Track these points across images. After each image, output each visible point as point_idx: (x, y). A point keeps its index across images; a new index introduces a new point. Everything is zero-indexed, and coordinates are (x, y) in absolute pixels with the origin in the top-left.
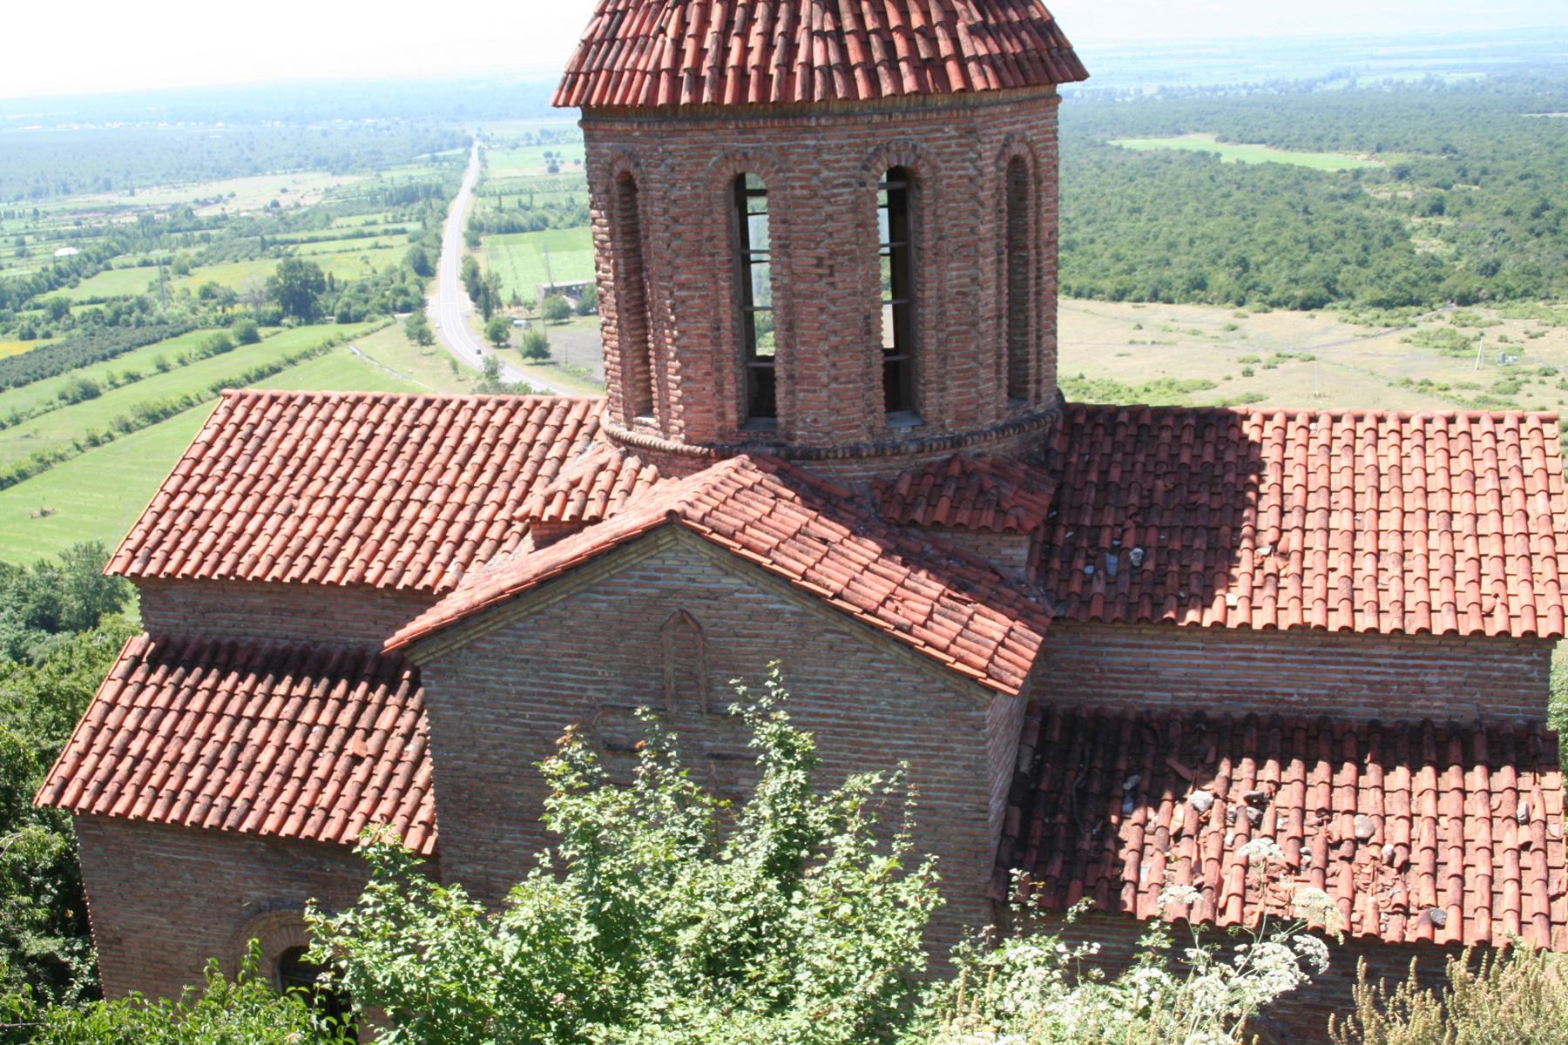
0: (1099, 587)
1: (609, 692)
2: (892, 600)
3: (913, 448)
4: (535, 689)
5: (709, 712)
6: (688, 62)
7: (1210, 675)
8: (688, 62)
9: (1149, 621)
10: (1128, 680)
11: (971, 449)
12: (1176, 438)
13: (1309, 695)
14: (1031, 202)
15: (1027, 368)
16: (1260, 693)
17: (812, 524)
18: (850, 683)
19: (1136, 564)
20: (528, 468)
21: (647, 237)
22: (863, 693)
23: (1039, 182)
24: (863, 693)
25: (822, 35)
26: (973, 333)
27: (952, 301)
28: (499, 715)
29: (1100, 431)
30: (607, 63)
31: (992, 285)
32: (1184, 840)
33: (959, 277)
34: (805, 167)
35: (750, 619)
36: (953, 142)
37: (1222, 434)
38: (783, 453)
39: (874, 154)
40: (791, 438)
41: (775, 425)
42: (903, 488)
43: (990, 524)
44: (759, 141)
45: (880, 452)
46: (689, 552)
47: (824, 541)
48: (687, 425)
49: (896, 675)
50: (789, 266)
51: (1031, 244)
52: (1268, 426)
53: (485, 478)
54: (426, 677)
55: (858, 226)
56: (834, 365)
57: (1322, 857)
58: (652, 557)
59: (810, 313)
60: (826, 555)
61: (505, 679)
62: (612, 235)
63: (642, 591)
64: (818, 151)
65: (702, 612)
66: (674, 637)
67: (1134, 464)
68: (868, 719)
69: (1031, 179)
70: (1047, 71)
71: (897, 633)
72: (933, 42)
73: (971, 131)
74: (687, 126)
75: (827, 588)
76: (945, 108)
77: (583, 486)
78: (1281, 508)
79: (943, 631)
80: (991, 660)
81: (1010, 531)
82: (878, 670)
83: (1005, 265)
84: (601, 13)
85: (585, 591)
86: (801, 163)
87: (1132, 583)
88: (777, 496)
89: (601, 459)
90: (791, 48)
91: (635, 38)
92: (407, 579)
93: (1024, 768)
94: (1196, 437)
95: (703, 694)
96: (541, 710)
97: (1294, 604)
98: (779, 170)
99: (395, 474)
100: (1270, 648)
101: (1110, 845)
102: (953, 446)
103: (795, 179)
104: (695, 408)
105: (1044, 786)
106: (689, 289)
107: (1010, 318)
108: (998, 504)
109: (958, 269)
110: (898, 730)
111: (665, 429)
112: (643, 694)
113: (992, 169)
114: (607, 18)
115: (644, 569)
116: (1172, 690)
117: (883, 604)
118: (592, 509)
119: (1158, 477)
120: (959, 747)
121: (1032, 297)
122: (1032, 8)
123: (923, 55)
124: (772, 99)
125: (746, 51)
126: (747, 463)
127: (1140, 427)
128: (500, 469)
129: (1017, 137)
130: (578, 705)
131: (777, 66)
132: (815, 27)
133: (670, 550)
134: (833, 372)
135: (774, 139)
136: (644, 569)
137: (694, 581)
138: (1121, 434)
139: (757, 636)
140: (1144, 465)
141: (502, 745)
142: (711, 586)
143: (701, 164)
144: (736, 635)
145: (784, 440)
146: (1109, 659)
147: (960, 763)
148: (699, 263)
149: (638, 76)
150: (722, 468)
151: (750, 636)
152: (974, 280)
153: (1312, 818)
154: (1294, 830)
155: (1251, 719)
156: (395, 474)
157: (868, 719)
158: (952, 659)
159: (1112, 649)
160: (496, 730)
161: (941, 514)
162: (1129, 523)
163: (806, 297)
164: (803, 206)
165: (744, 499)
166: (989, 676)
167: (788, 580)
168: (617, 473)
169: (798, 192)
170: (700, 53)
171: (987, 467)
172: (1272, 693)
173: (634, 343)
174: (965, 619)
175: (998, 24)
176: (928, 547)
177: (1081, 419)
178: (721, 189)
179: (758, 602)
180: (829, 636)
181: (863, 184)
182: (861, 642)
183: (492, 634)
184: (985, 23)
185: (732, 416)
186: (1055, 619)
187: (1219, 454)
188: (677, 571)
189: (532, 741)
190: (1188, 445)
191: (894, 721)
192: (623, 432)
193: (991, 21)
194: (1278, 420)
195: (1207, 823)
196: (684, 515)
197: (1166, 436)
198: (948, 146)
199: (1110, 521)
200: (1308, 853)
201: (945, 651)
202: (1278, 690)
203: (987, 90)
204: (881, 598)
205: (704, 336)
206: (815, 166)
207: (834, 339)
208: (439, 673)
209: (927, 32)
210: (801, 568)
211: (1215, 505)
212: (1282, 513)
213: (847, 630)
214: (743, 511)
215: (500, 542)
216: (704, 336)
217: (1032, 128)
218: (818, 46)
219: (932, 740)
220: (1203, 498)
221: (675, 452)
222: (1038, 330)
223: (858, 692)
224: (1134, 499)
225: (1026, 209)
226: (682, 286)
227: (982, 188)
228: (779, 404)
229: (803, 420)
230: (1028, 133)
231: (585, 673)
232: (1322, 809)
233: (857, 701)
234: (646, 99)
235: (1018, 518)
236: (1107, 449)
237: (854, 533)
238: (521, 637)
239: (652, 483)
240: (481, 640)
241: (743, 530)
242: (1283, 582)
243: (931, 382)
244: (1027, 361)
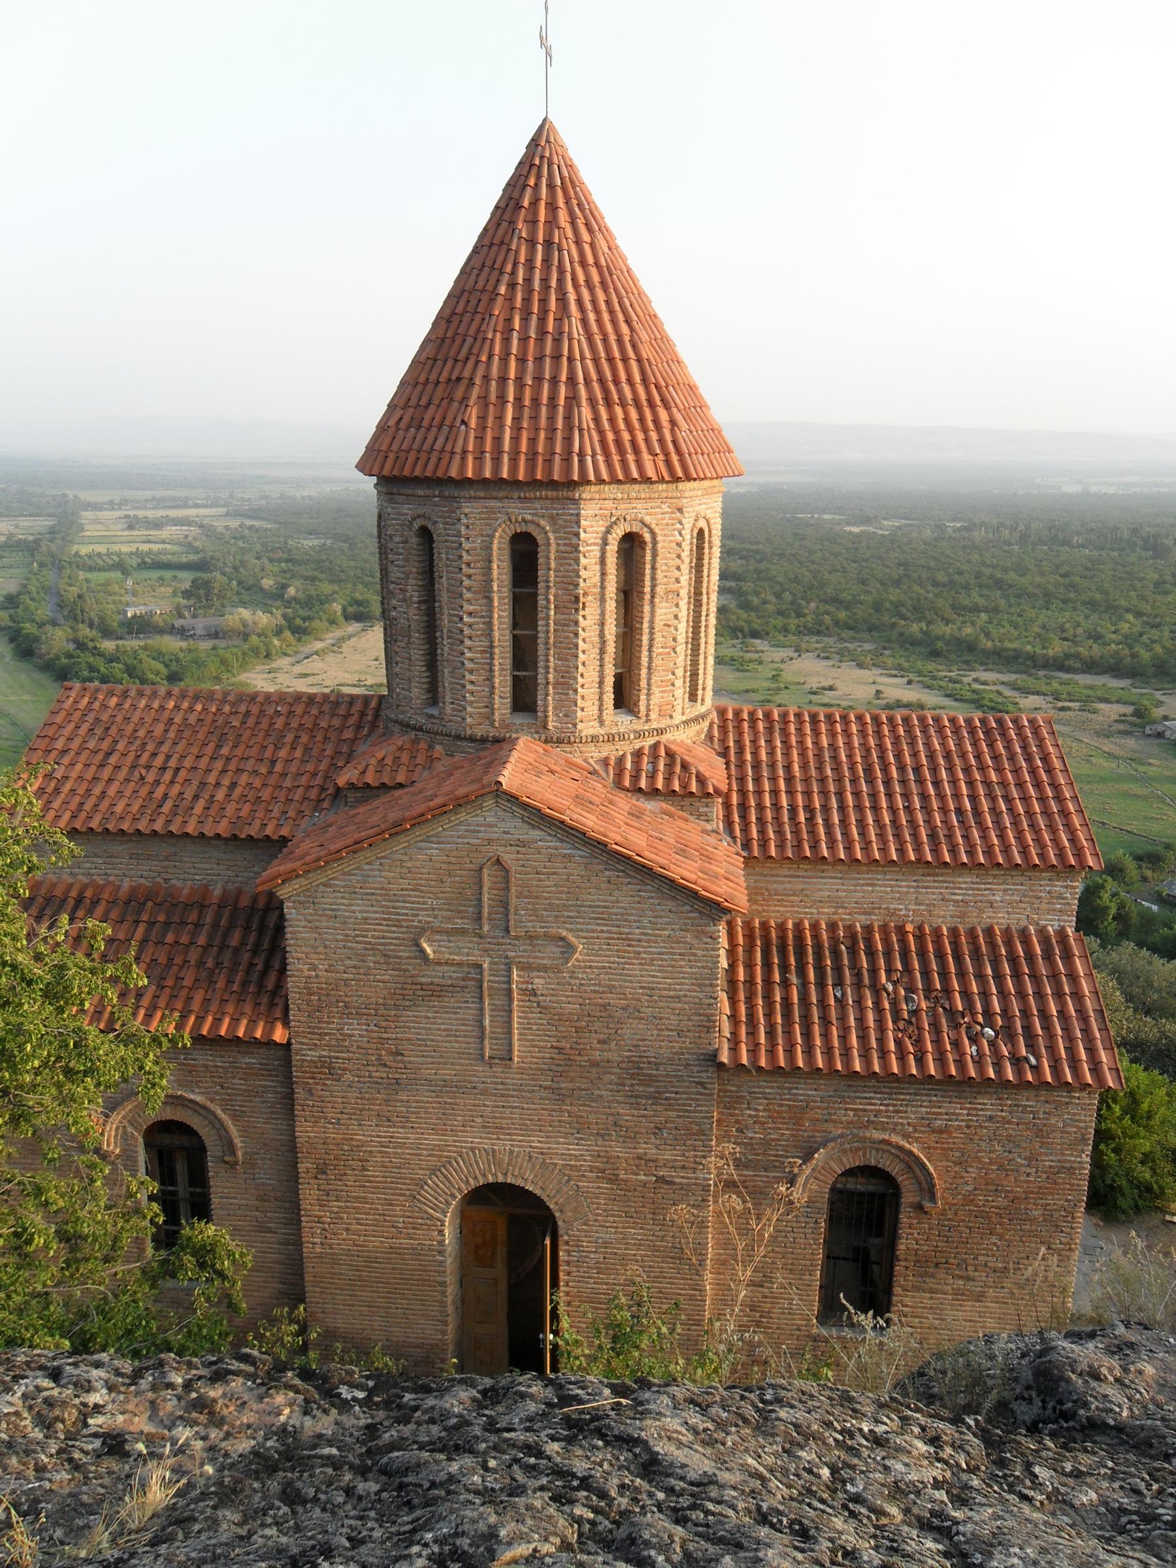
13: (913, 911)
16: (880, 908)
22: (631, 915)
28: (346, 935)
31: (685, 619)
51: (704, 591)
59: (567, 638)
96: (382, 931)
135: (547, 509)
137: (504, 832)
139: (554, 873)
144: (537, 873)
146: (775, 886)
169: (562, 548)
180: (607, 873)
183: (344, 874)
189: (374, 955)
202: (892, 906)
223: (627, 914)
231: (418, 903)
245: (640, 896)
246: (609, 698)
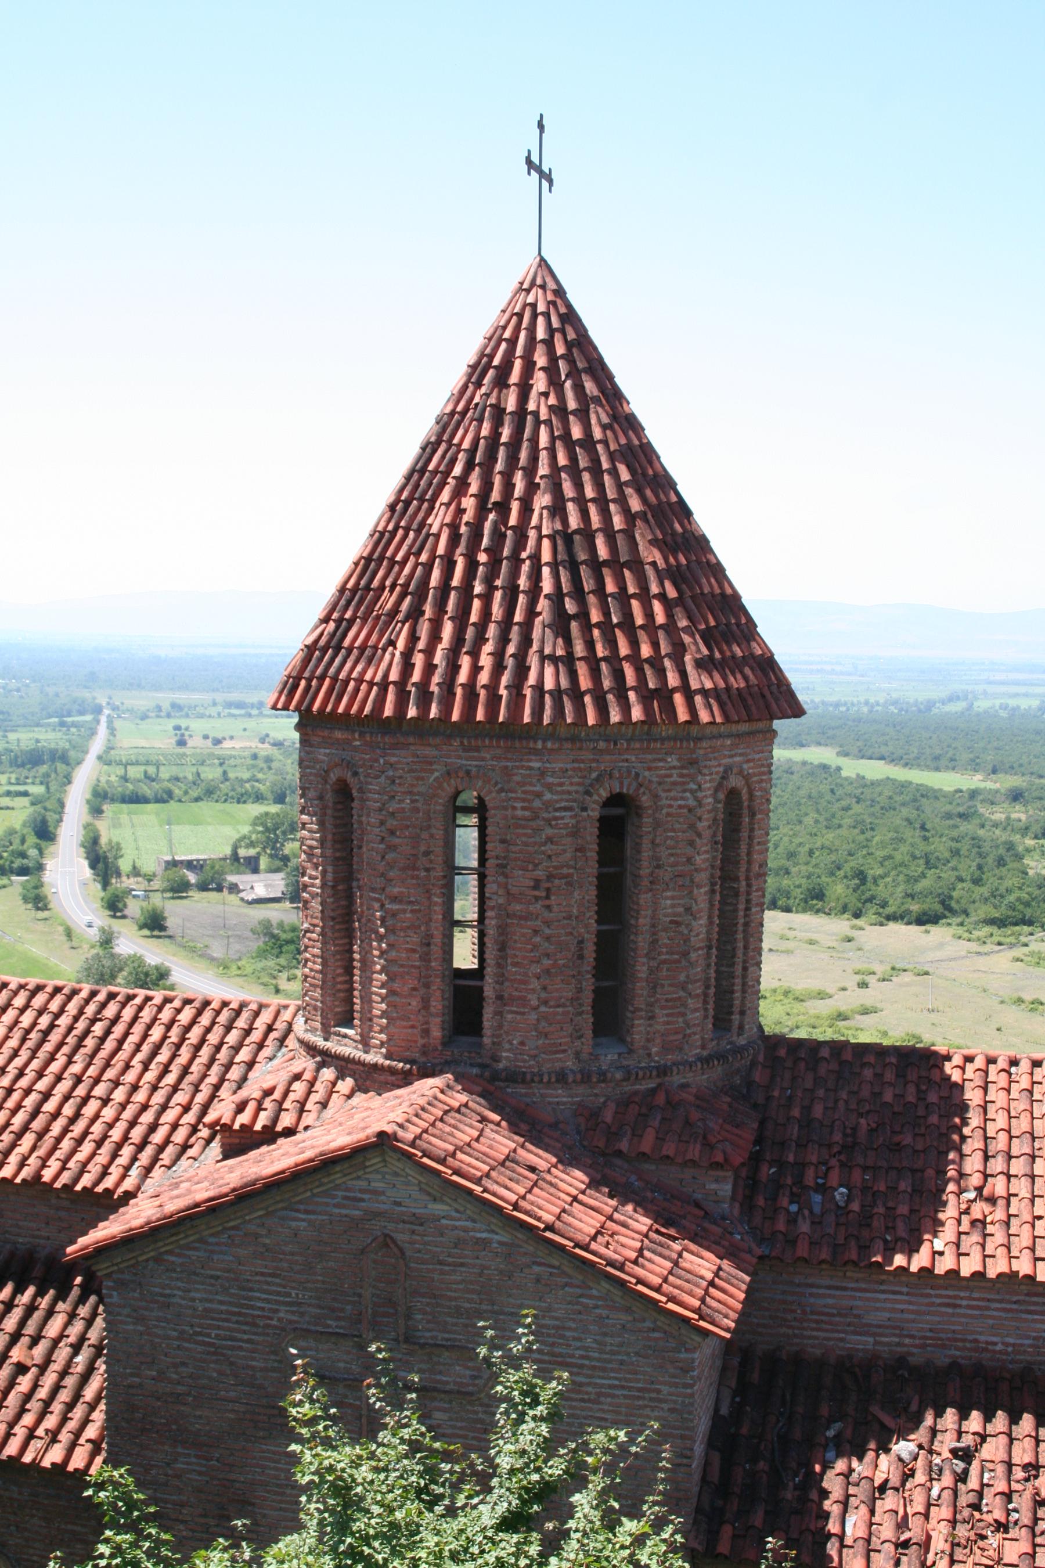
0: (804, 1227)
1: (302, 1314)
2: (602, 1234)
3: (618, 1076)
4: (224, 1308)
5: (407, 1340)
6: (416, 677)
7: (913, 1321)
8: (416, 677)
9: (855, 1264)
10: (830, 1323)
11: (676, 1079)
12: (878, 1076)
13: (1014, 1345)
14: (745, 834)
15: (732, 999)
16: (964, 1341)
17: (520, 1151)
18: (556, 1319)
19: (842, 1204)
20: (215, 1070)
21: (360, 847)
22: (570, 1329)
23: (752, 815)
24: (570, 1329)
25: (553, 659)
26: (684, 963)
27: (665, 930)
28: (183, 1332)
29: (802, 1065)
30: (332, 671)
32: (889, 1492)
33: (673, 906)
34: (528, 788)
35: (456, 1247)
36: (674, 771)
37: (923, 1074)
38: (487, 1074)
39: (597, 779)
40: (496, 1059)
41: (480, 1045)
42: (608, 1116)
43: (697, 1158)
44: (483, 759)
45: (585, 1078)
46: (396, 1174)
47: (532, 1169)
48: (389, 1040)
49: (605, 1312)
50: (505, 886)
51: (742, 875)
52: (970, 1068)
53: (170, 1079)
54: (109, 1288)
55: (577, 850)
56: (545, 988)
57: (1030, 1515)
58: (358, 1178)
59: (524, 935)
60: (535, 1184)
61: (193, 1294)
62: (322, 842)
63: (344, 1211)
64: (542, 773)
65: (406, 1237)
66: (375, 1261)
67: (836, 1101)
68: (573, 1356)
69: (746, 811)
70: (768, 707)
71: (608, 1269)
72: (661, 673)
73: (693, 762)
74: (411, 740)
75: (539, 1219)
76: (668, 738)
77: (277, 1095)
78: (985, 1152)
79: (654, 1270)
80: (703, 1301)
81: (718, 1166)
82: (586, 1306)
83: (718, 897)
84: (326, 620)
85: (285, 1209)
86: (524, 784)
87: (838, 1224)
88: (483, 1119)
89: (296, 1067)
90: (522, 670)
91: (363, 648)
92: (86, 1181)
93: (724, 1411)
94: (897, 1076)
95: (401, 1322)
96: (229, 1329)
97: (1001, 1252)
98: (502, 790)
99: (76, 1068)
100: (976, 1295)
101: (814, 1495)
102: (658, 1076)
103: (516, 799)
104: (398, 1023)
105: (744, 1431)
106: (401, 902)
107: (718, 949)
108: (705, 1137)
109: (673, 898)
110: (604, 1369)
111: (365, 1043)
112: (338, 1319)
113: (710, 800)
114: (332, 625)
115: (348, 1190)
116: (874, 1335)
117: (594, 1238)
118: (286, 1120)
119: (861, 1115)
120: (665, 1389)
121: (741, 928)
122: (754, 644)
123: (651, 685)
124: (501, 719)
125: (476, 669)
126: (452, 1083)
127: (841, 1063)
128: (185, 1071)
129: (735, 770)
130: (268, 1326)
131: (506, 687)
132: (547, 651)
133: (377, 1171)
134: (543, 995)
135: (498, 758)
136: (348, 1190)
137: (399, 1204)
138: (822, 1069)
139: (462, 1265)
140: (846, 1102)
141: (184, 1364)
142: (417, 1211)
143: (422, 779)
144: (441, 1263)
145: (489, 1061)
146: (812, 1300)
147: (665, 1406)
148: (413, 878)
149: (364, 687)
150: (428, 1086)
151: (455, 1265)
152: (688, 910)
153: (1019, 1474)
154: (1001, 1486)
155: (954, 1366)
156: (76, 1068)
157: (573, 1356)
158: (664, 1299)
159: (814, 1290)
160: (179, 1347)
161: (646, 1145)
162: (834, 1162)
163: (521, 918)
164: (524, 827)
165: (453, 1122)
166: (701, 1318)
167: (500, 1209)
168: (312, 1083)
169: (519, 813)
170: (430, 668)
171: (691, 1098)
172: (976, 1341)
173: (337, 952)
174: (675, 1256)
175: (723, 658)
176: (633, 1178)
177: (782, 1052)
178: (439, 805)
179: (466, 1230)
180: (537, 1269)
181: (584, 809)
182: (570, 1277)
184: (711, 657)
185: (436, 1033)
186: (761, 1258)
187: (921, 1096)
188: (383, 1193)
189: (216, 1362)
190: (890, 1084)
191: (599, 1360)
192: (320, 1042)
193: (717, 655)
194: (979, 1062)
195: (912, 1475)
196: (395, 1137)
197: (868, 1073)
198: (670, 776)
199: (814, 1159)
200: (1016, 1510)
201: (658, 1289)
202: (982, 1338)
203: (713, 723)
204: (593, 1231)
205: (414, 951)
206: (538, 788)
207: (546, 962)
208: (121, 1284)
209: (656, 662)
210: (513, 1198)
211: (919, 1147)
212: (986, 1158)
213: (557, 1263)
214: (452, 1135)
215: (185, 1147)
216: (414, 951)
217: (748, 761)
218: (549, 671)
219: (638, 1381)
220: (907, 1139)
221: (375, 1066)
222: (745, 962)
223: (564, 1328)
224: (837, 1137)
225: (739, 840)
226: (394, 899)
227: (700, 819)
228: (486, 1024)
229: (510, 1042)
230: (745, 766)
231: (279, 1294)
232: (1029, 1464)
233: (563, 1337)
234: (372, 711)
235: (724, 1152)
236: (809, 1084)
237: (560, 1161)
238: (212, 1252)
239: (349, 1097)
240: (170, 1252)
241: (453, 1155)
242: (990, 1229)
243: (641, 1010)
244: (732, 992)
245: (581, 1304)
246: (587, 1020)
